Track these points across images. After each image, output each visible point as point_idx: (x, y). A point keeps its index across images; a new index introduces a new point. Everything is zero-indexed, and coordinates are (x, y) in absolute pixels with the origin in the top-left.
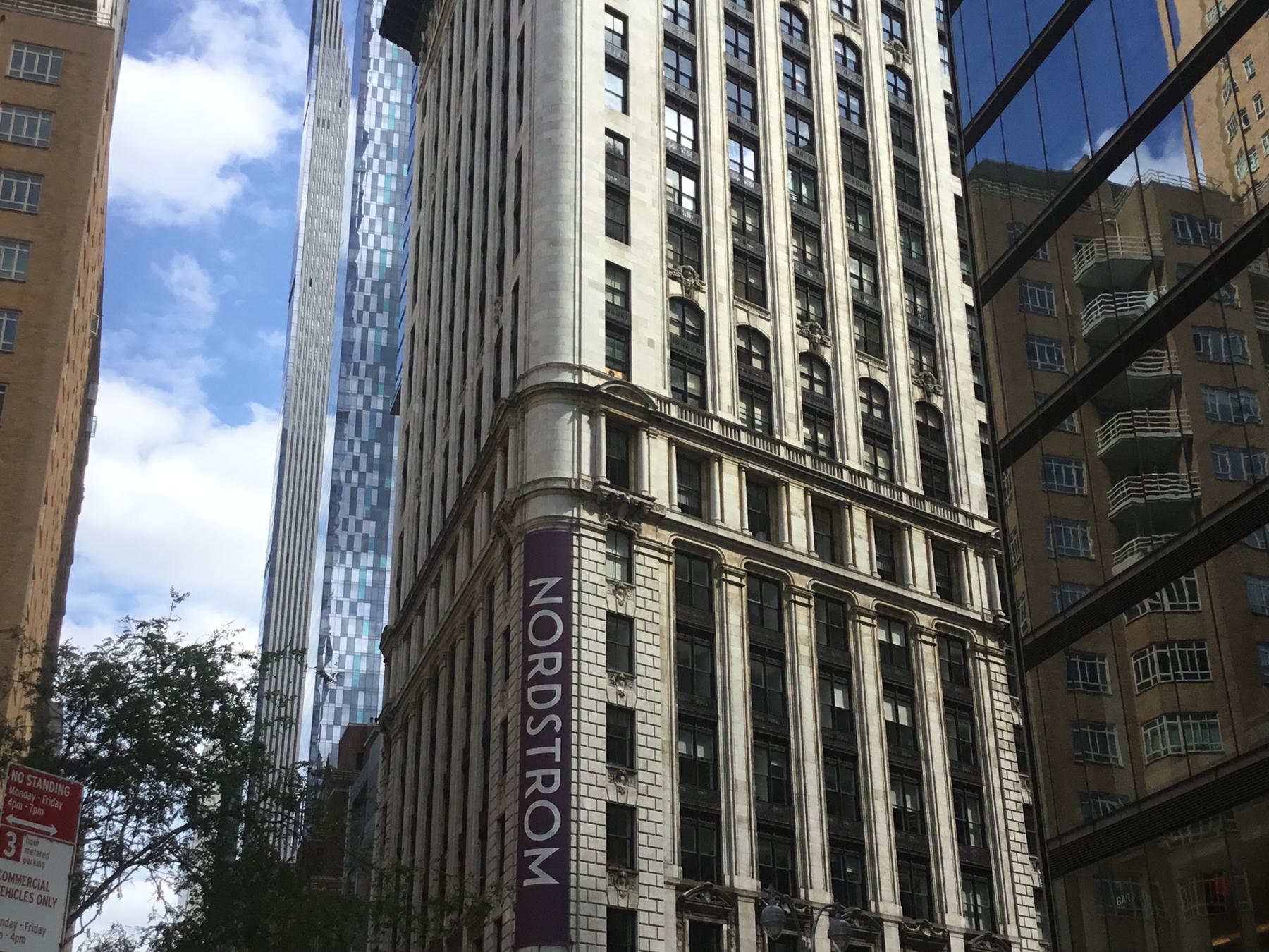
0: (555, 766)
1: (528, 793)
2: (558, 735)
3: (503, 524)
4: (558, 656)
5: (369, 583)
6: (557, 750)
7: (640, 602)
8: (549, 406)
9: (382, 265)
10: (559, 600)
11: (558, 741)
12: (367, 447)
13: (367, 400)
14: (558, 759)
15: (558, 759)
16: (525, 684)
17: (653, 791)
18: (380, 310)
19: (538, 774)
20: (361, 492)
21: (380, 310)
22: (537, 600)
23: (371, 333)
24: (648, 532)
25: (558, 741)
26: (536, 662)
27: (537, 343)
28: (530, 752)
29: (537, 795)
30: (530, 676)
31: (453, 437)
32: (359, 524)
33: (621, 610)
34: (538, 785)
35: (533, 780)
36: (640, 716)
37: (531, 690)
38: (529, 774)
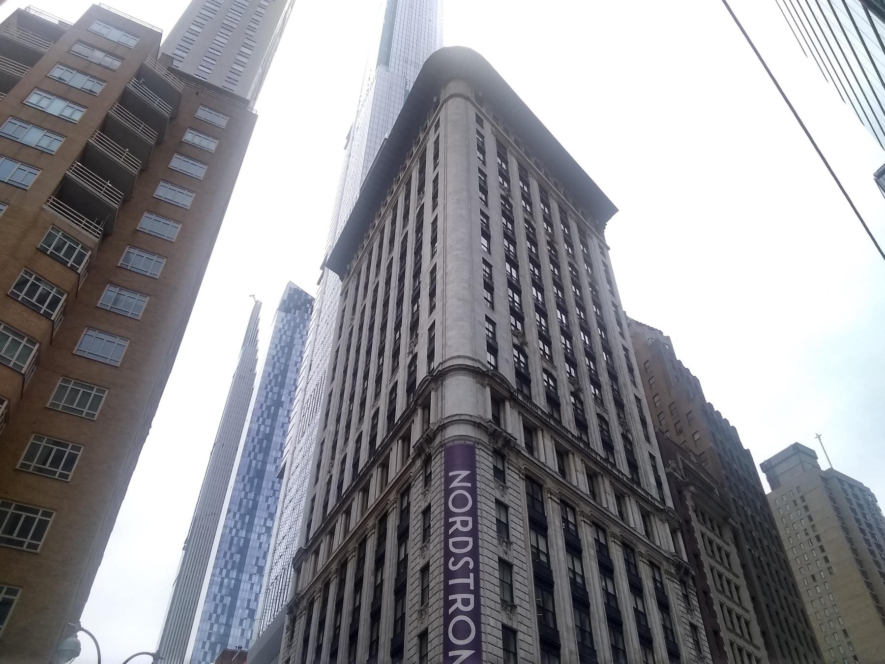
0: (471, 592)
1: (450, 611)
2: (472, 571)
3: (425, 446)
4: (470, 519)
5: (232, 587)
6: (471, 581)
7: (512, 498)
8: (460, 377)
9: (264, 432)
10: (469, 485)
11: (472, 575)
12: (242, 517)
13: (246, 494)
14: (472, 588)
15: (472, 588)
16: (447, 536)
17: (526, 621)
18: (260, 452)
19: (459, 597)
20: (236, 539)
21: (260, 452)
22: (455, 484)
23: (254, 462)
24: (513, 458)
25: (472, 575)
26: (455, 522)
27: (450, 346)
28: (451, 582)
29: (458, 612)
30: (450, 532)
31: (366, 427)
32: (232, 555)
33: (502, 499)
34: (459, 605)
35: (455, 601)
36: (515, 569)
37: (451, 541)
38: (451, 597)
